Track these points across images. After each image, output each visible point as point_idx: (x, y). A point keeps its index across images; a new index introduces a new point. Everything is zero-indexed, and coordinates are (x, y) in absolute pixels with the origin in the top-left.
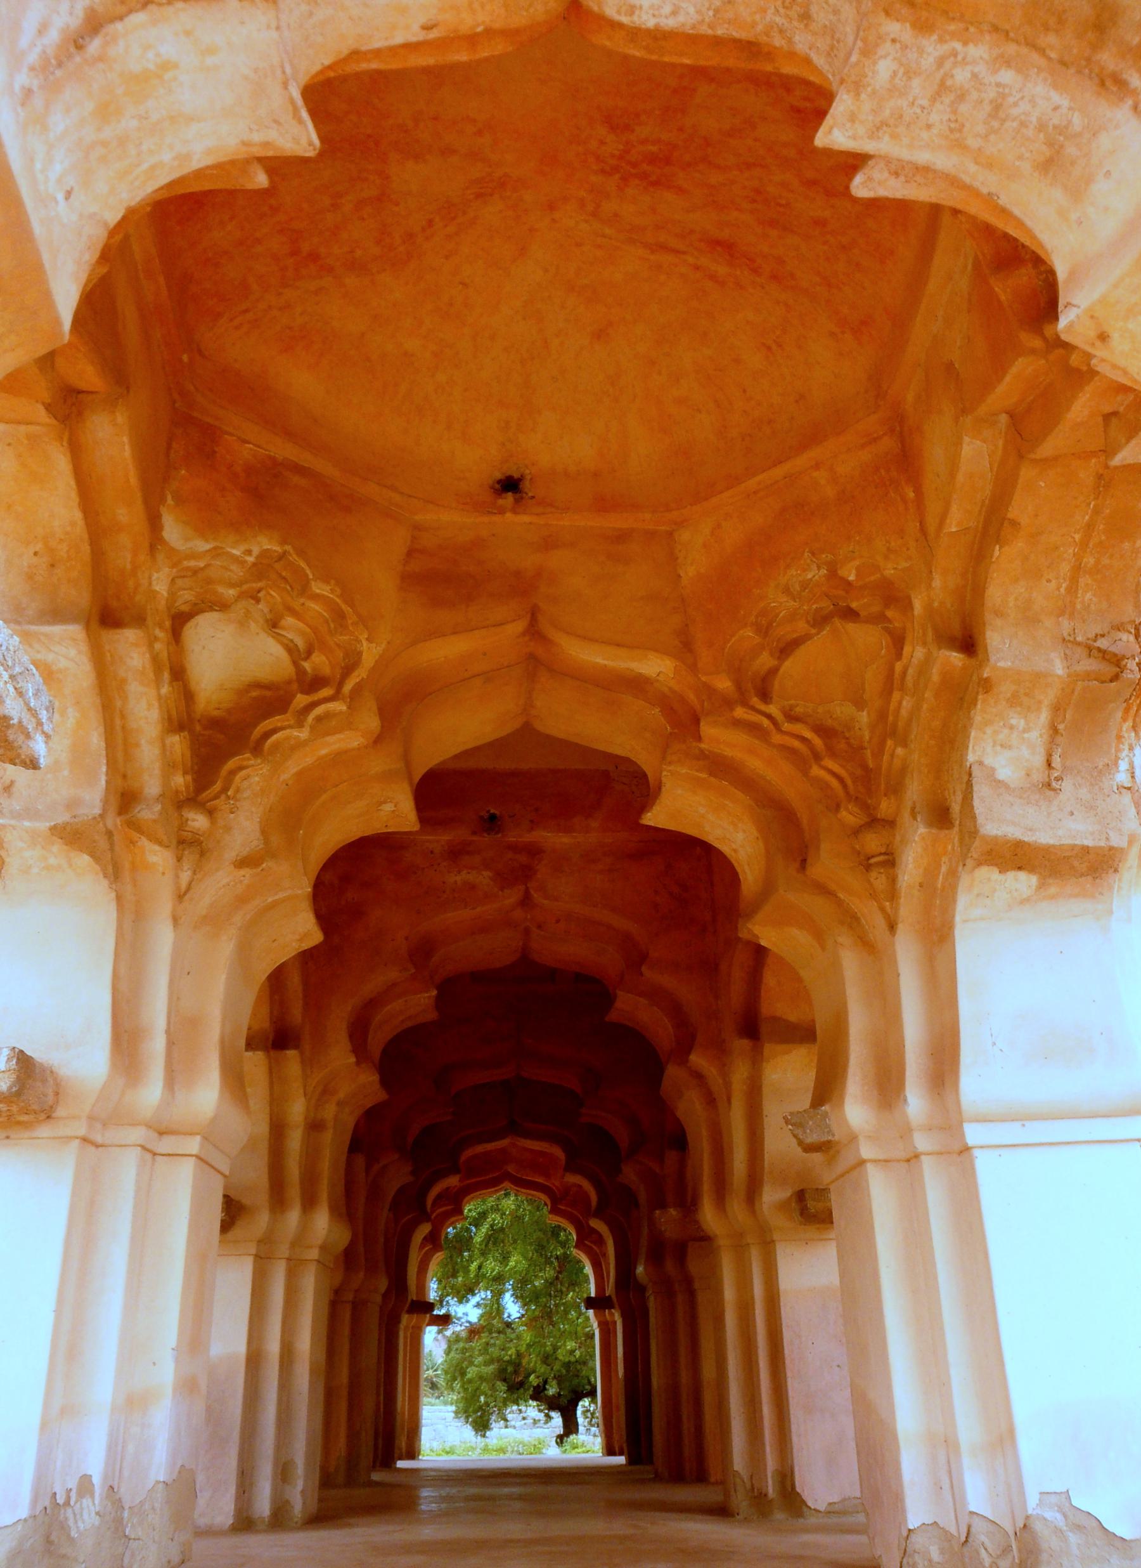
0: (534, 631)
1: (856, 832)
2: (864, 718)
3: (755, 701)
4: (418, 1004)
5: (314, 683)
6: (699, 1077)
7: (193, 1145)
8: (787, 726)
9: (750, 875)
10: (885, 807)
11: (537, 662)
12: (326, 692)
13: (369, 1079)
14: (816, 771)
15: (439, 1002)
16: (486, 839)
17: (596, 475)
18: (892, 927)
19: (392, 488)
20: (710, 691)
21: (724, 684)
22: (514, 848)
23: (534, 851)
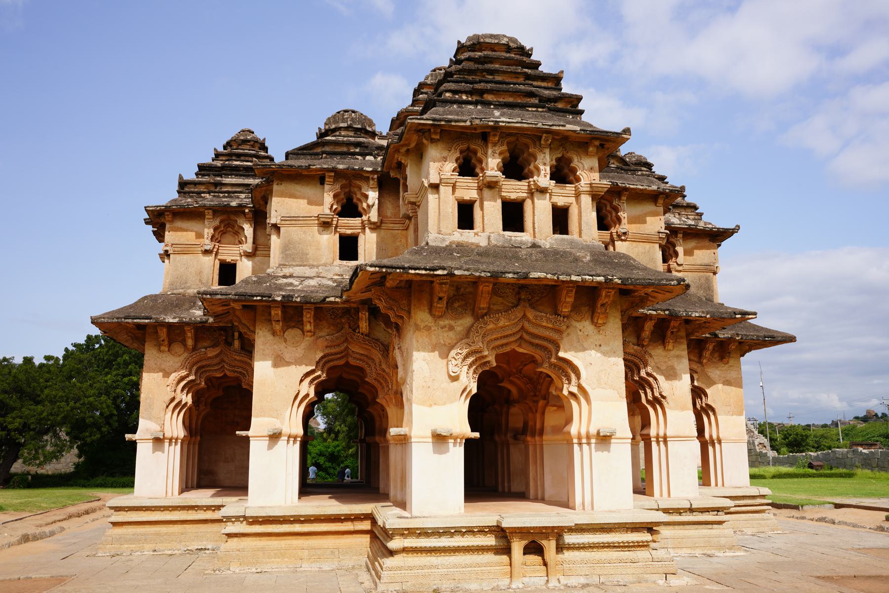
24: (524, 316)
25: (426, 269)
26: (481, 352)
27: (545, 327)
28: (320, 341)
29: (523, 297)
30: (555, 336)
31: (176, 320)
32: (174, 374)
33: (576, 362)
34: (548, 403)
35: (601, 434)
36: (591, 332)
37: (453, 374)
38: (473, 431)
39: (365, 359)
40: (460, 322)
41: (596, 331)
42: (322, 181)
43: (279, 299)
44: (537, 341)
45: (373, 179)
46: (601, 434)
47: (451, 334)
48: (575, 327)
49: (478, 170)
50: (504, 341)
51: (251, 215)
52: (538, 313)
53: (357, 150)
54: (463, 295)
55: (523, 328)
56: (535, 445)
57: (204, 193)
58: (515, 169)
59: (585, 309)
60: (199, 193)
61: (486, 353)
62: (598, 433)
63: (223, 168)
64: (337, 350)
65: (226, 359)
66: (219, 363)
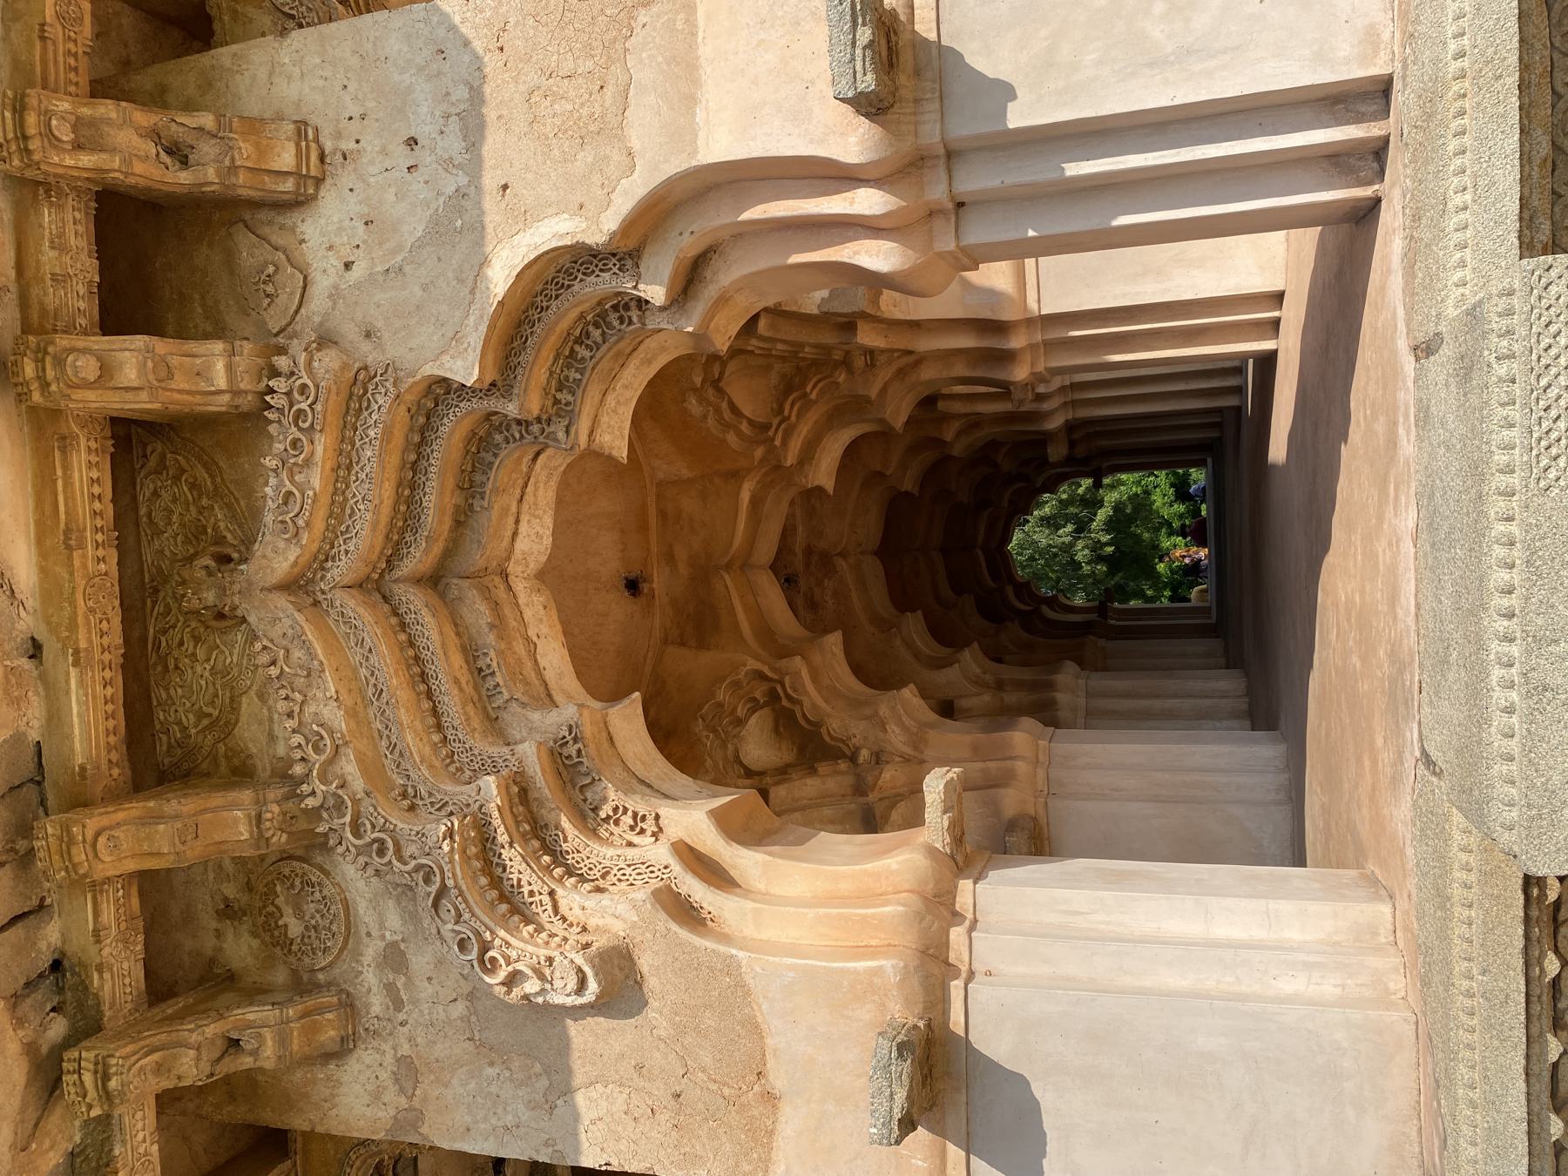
0: (728, 567)
1: (850, 371)
2: (777, 366)
3: (771, 433)
4: (914, 625)
5: (773, 697)
6: (959, 435)
7: (1041, 743)
8: (786, 413)
9: (866, 428)
10: (838, 355)
11: (743, 564)
12: (779, 689)
13: (966, 655)
14: (813, 396)
15: (913, 611)
16: (802, 583)
17: (623, 532)
18: (910, 353)
19: (645, 657)
20: (762, 461)
21: (759, 452)
22: (807, 565)
23: (809, 551)
24: (298, 586)
26: (482, 826)
27: (344, 465)
29: (210, 597)
30: (384, 413)
33: (500, 276)
34: (864, 315)
35: (868, 82)
36: (353, 205)
37: (593, 986)
38: (916, 819)
40: (363, 910)
41: (346, 178)
44: (436, 501)
46: (868, 82)
47: (420, 961)
48: (335, 295)
50: (447, 669)
52: (269, 518)
54: (249, 888)
55: (374, 585)
56: (1050, 346)
59: (249, 252)
61: (490, 784)
62: (870, 106)
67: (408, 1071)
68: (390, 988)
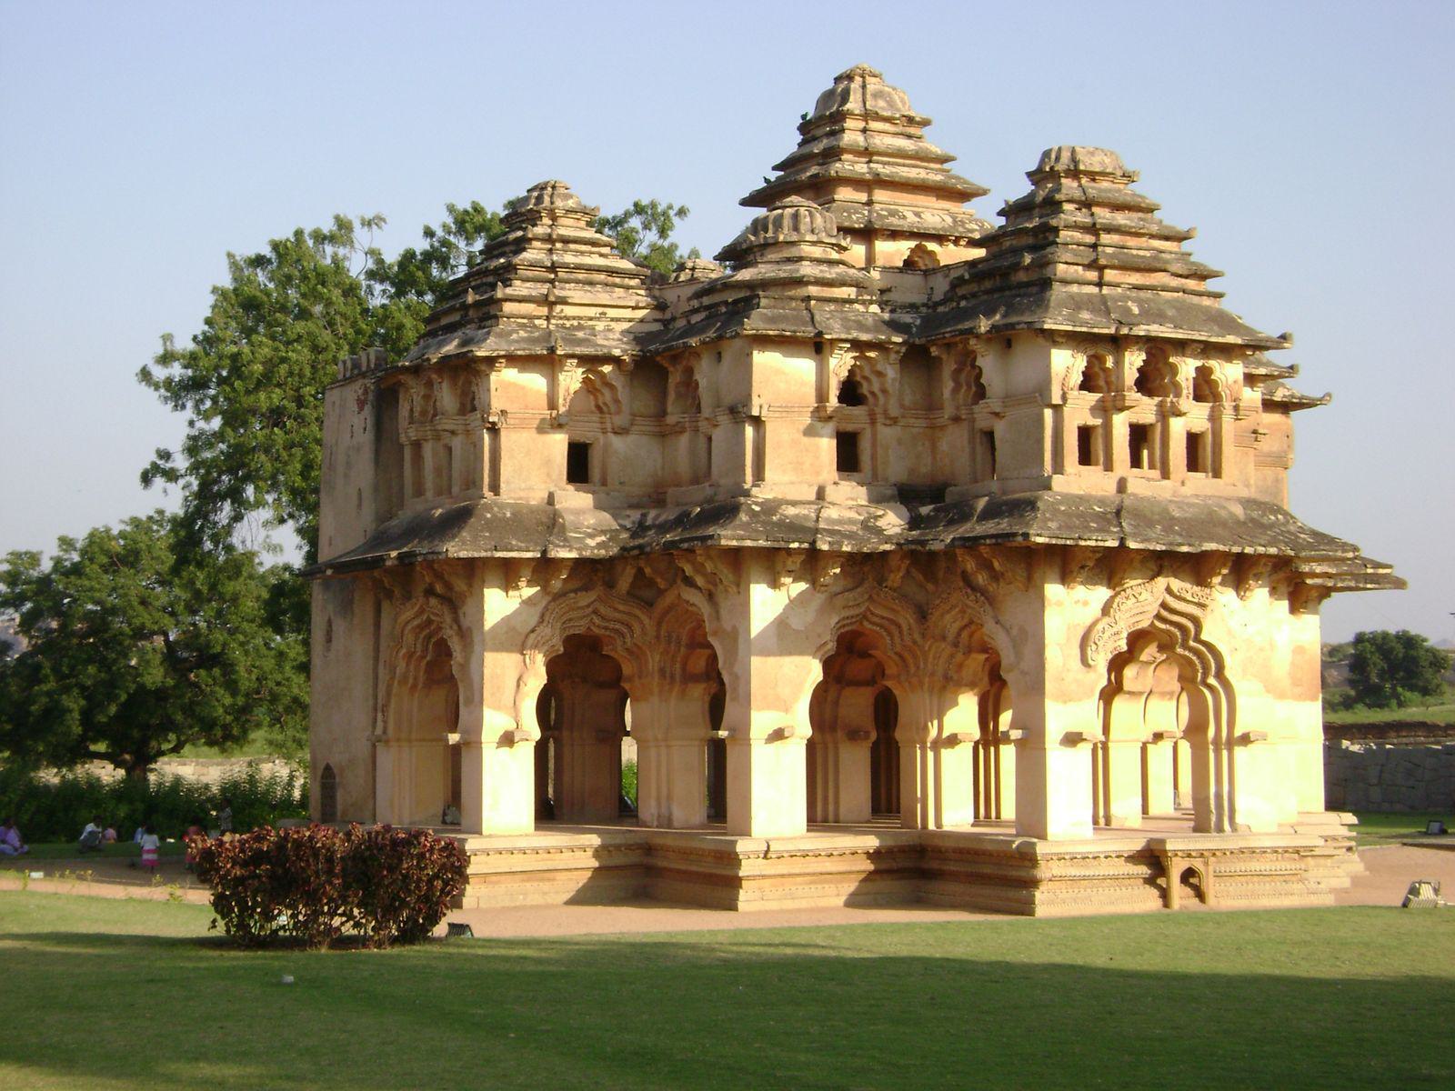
25: (1096, 540)
28: (840, 601)
31: (574, 555)
32: (533, 636)
39: (885, 623)
42: (818, 346)
43: (825, 547)
45: (898, 352)
49: (1102, 383)
51: (631, 367)
53: (850, 292)
57: (539, 318)
58: (1146, 383)
60: (531, 318)
63: (553, 268)
64: (857, 611)
65: (603, 610)
66: (588, 615)
67: (1059, 604)
68: (1077, 602)
